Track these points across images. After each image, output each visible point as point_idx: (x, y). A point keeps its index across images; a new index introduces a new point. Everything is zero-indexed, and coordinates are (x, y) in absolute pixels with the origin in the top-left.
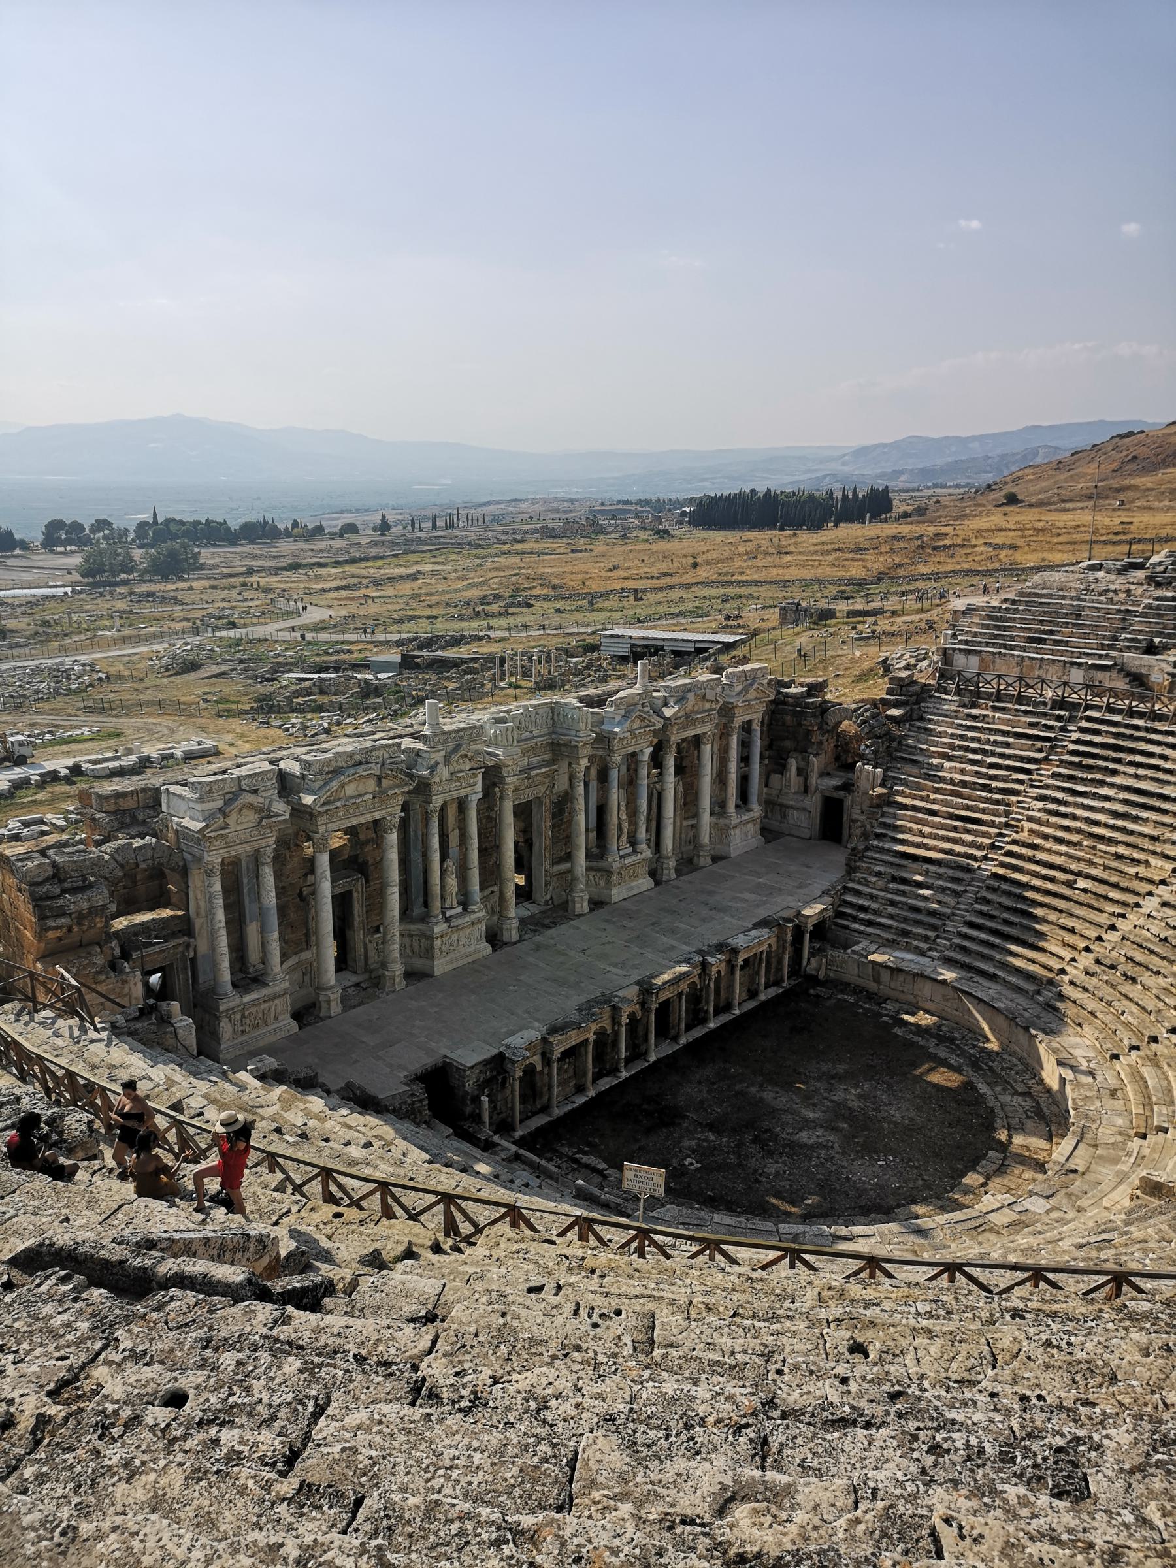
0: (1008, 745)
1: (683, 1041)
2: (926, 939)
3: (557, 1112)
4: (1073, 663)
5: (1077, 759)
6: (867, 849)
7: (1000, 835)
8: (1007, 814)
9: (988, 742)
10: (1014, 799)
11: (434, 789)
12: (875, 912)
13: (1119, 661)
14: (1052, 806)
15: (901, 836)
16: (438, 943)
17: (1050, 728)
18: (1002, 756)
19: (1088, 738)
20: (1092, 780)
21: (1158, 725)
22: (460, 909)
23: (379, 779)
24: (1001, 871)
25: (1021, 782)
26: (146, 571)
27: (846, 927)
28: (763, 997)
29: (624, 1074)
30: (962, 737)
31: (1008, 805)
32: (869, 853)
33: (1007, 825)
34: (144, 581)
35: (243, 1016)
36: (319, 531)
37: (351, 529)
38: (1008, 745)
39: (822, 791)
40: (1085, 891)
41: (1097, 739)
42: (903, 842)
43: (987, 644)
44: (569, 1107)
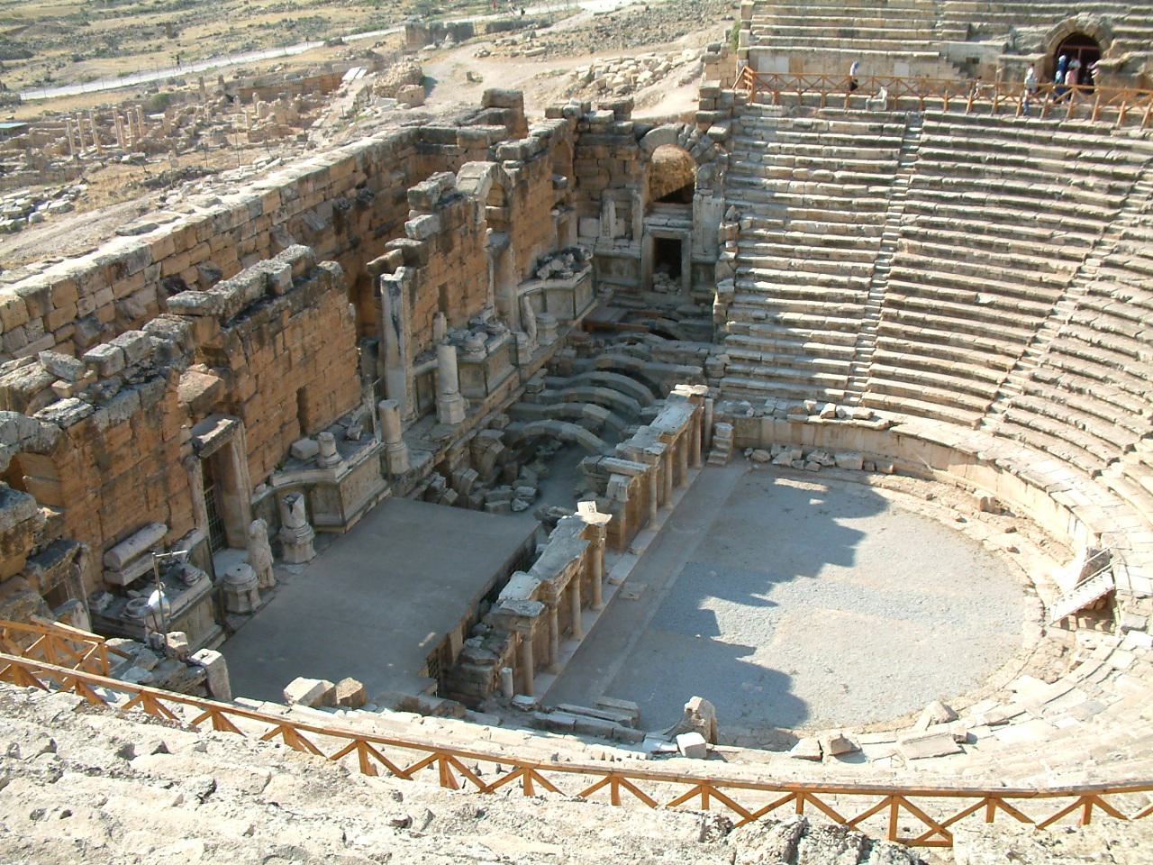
4: (896, 57)
5: (935, 163)
7: (880, 257)
8: (879, 233)
9: (830, 154)
10: (881, 214)
12: (768, 364)
13: (944, 51)
14: (923, 218)
17: (893, 132)
18: (850, 168)
19: (939, 138)
20: (958, 184)
21: (1005, 118)
24: (895, 297)
25: (882, 195)
30: (800, 152)
31: (876, 222)
32: (740, 298)
33: (883, 246)
38: (853, 155)
39: (652, 234)
40: (990, 305)
41: (948, 139)
43: (795, 43)
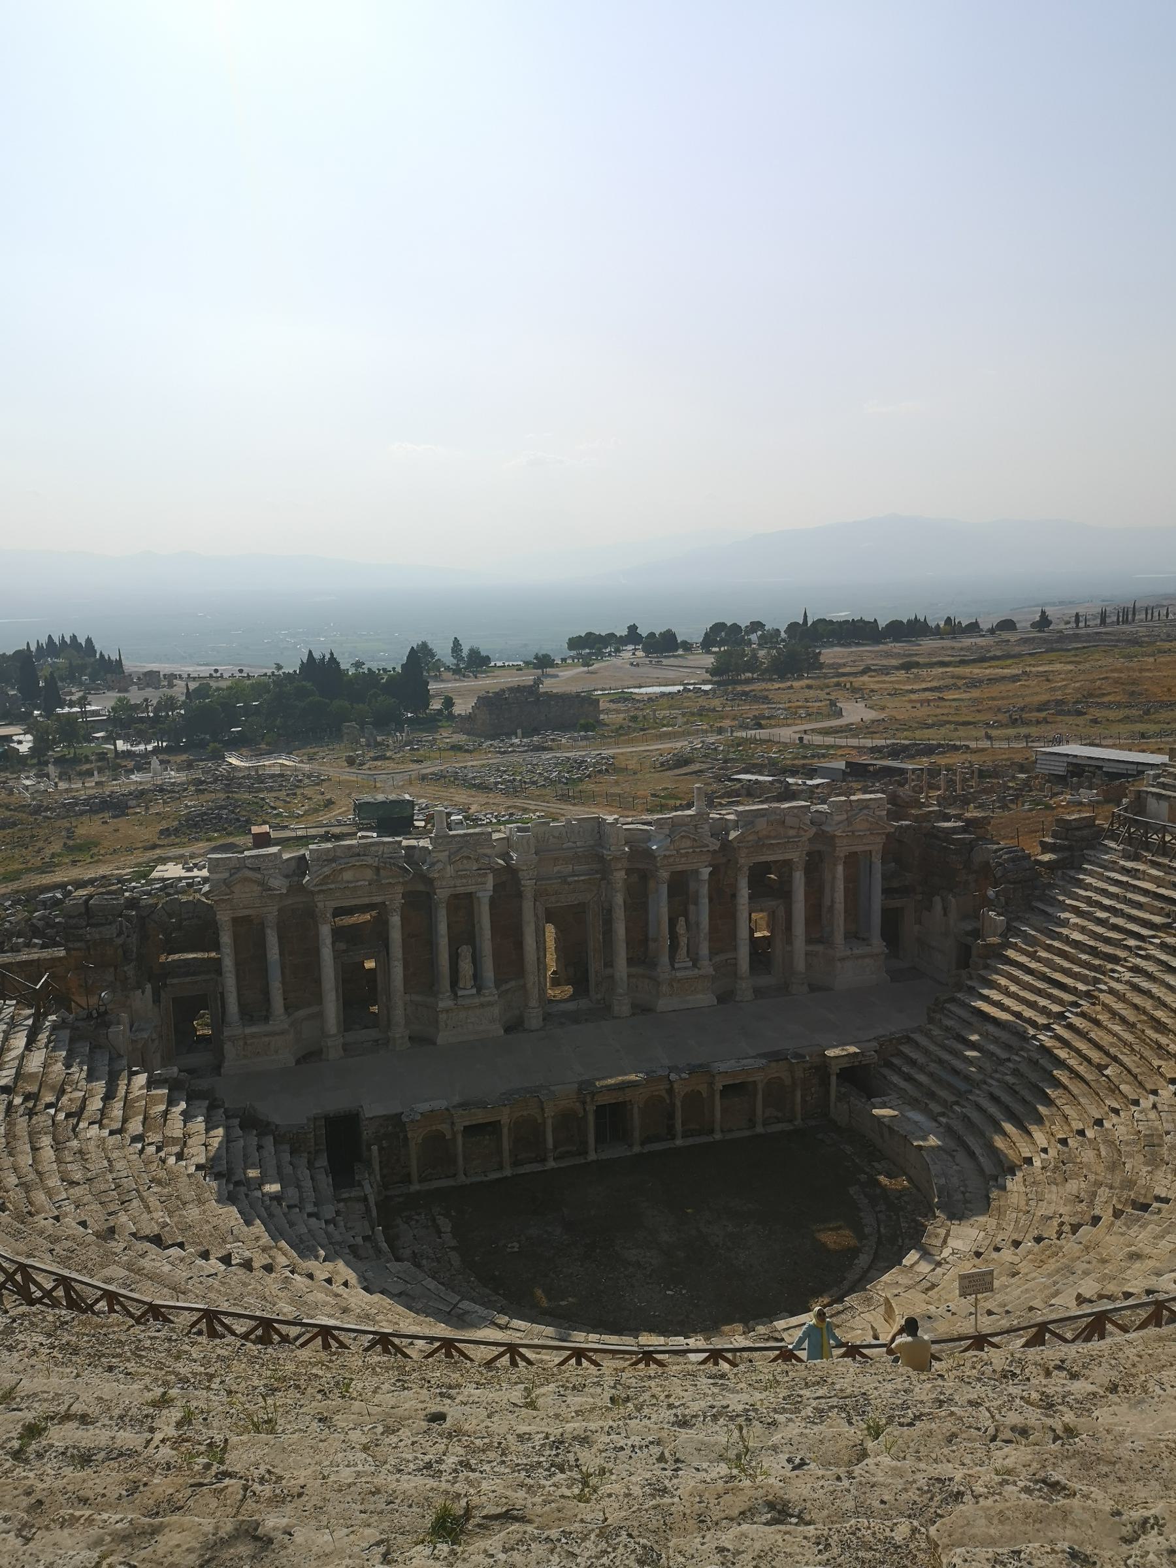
0: (1139, 906)
1: (637, 1149)
2: (944, 1103)
3: (462, 1179)
6: (953, 1000)
11: (437, 884)
15: (986, 992)
16: (443, 1017)
22: (474, 991)
23: (378, 869)
26: (766, 670)
27: (885, 1077)
28: (760, 1129)
29: (551, 1164)
33: (1088, 995)
34: (763, 680)
35: (245, 1043)
36: (974, 628)
37: (1008, 625)
38: (1139, 906)
42: (986, 999)
44: (478, 1179)
